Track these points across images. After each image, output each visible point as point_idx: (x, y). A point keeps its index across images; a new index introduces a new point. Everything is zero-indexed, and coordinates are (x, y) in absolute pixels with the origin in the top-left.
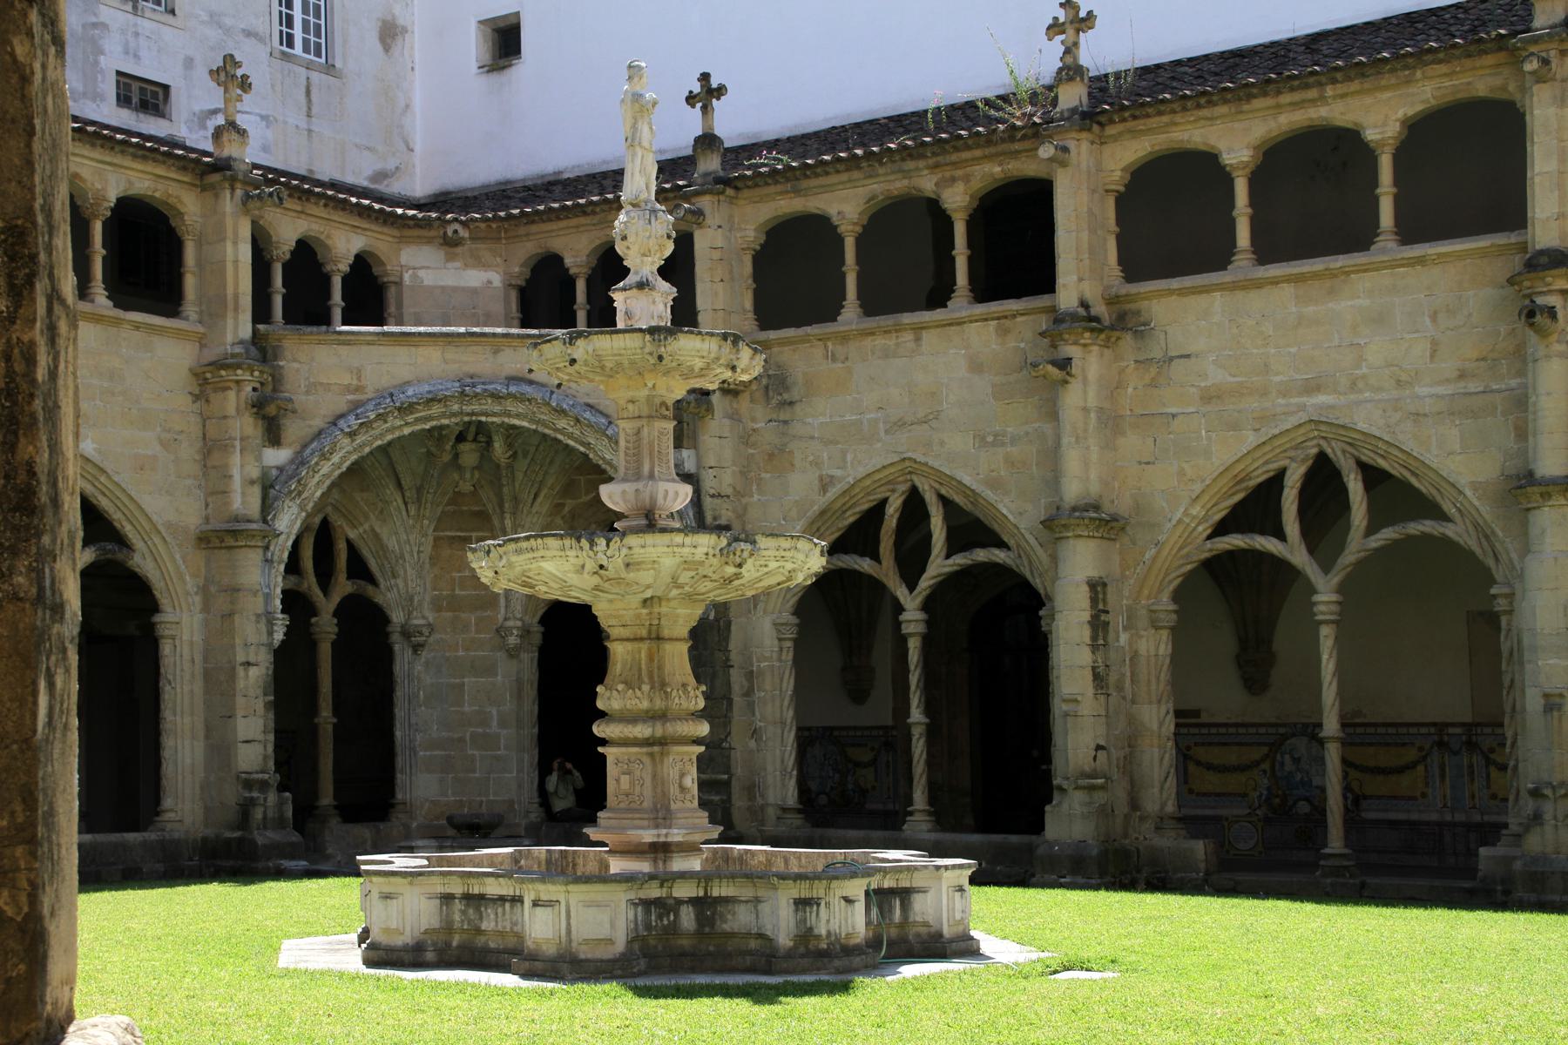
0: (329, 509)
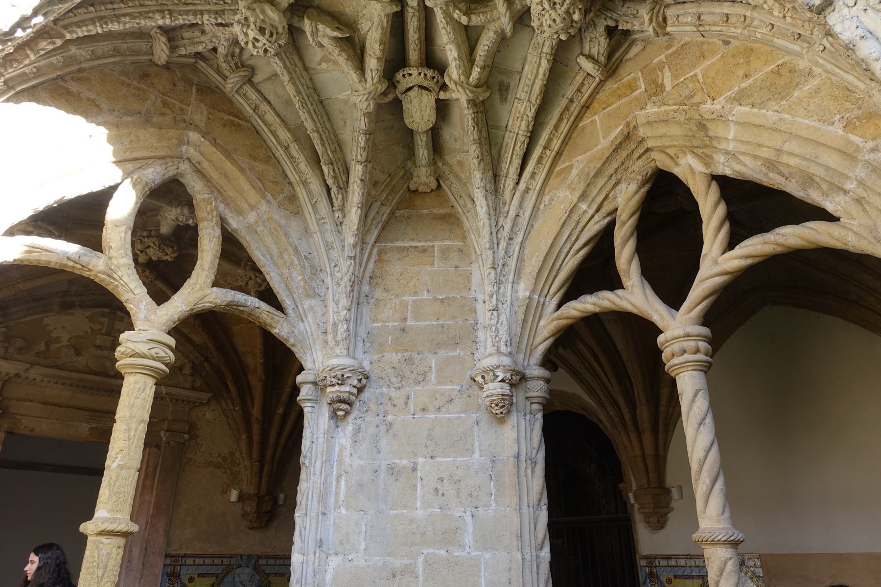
0: (185, 167)
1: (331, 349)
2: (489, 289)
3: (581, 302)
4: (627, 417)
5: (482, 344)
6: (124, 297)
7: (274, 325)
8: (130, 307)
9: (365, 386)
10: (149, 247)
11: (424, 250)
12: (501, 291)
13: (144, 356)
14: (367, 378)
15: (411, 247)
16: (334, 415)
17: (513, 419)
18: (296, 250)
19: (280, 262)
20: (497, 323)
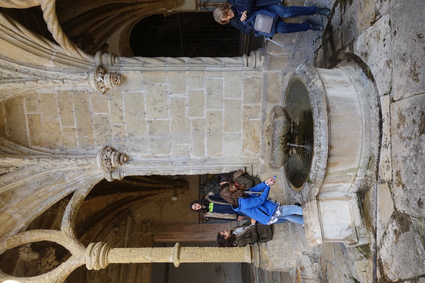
1: (92, 166)
2: (50, 84)
3: (53, 32)
4: (129, 8)
5: (84, 88)
6: (68, 273)
7: (81, 196)
8: (73, 269)
9: (111, 148)
10: (47, 262)
11: (31, 120)
12: (51, 77)
13: (98, 257)
14: (107, 147)
15: (29, 127)
16: (127, 162)
17: (123, 72)
18: (36, 190)
19: (44, 198)
20: (70, 79)
